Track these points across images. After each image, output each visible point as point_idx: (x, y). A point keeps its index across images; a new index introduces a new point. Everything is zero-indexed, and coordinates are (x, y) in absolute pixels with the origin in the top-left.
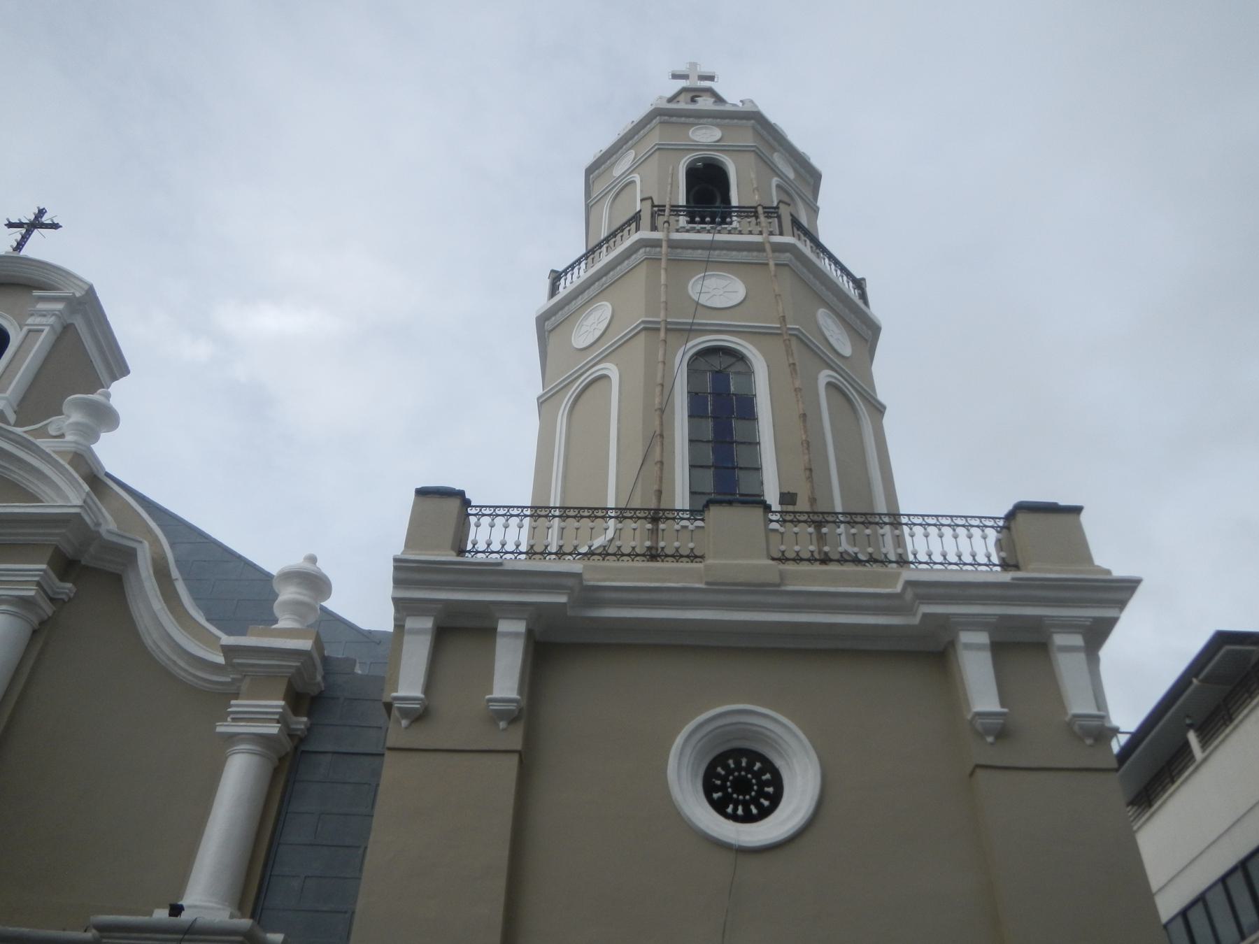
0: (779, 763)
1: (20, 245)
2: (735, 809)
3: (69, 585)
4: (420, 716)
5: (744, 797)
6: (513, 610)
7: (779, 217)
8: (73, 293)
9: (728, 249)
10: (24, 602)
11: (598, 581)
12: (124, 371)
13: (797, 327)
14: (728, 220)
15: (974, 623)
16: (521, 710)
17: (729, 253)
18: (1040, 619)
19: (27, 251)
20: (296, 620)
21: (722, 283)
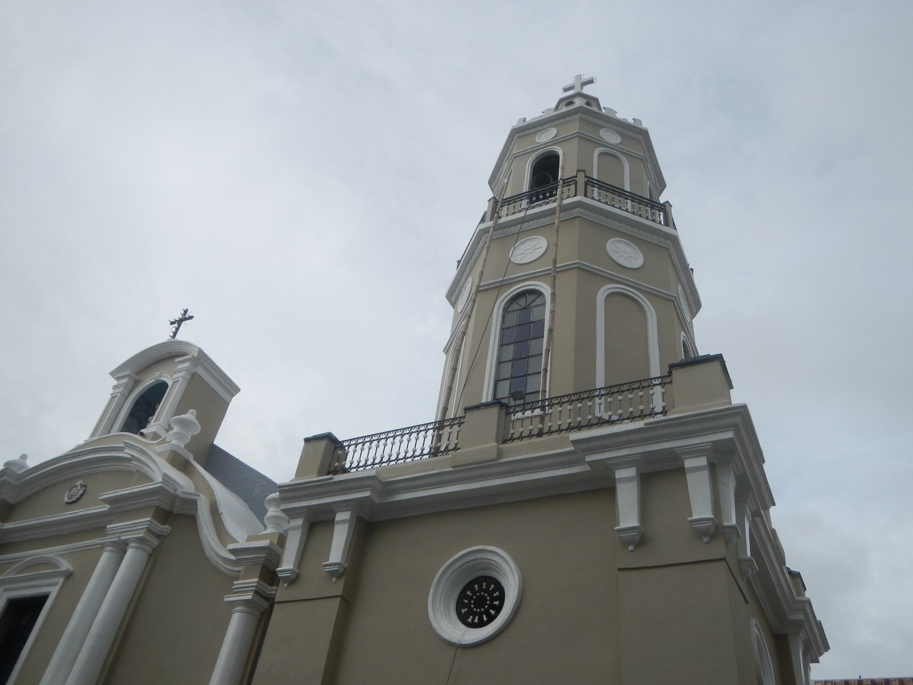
0: (504, 583)
1: (175, 334)
2: (474, 619)
3: (166, 526)
4: (294, 579)
5: (480, 610)
6: (343, 506)
7: (576, 183)
8: (193, 355)
9: (537, 218)
10: (140, 540)
11: (394, 477)
12: (237, 390)
13: (577, 261)
14: (554, 192)
15: (624, 463)
16: (345, 569)
17: (538, 220)
18: (671, 450)
19: (179, 337)
20: (273, 528)
21: (532, 243)
